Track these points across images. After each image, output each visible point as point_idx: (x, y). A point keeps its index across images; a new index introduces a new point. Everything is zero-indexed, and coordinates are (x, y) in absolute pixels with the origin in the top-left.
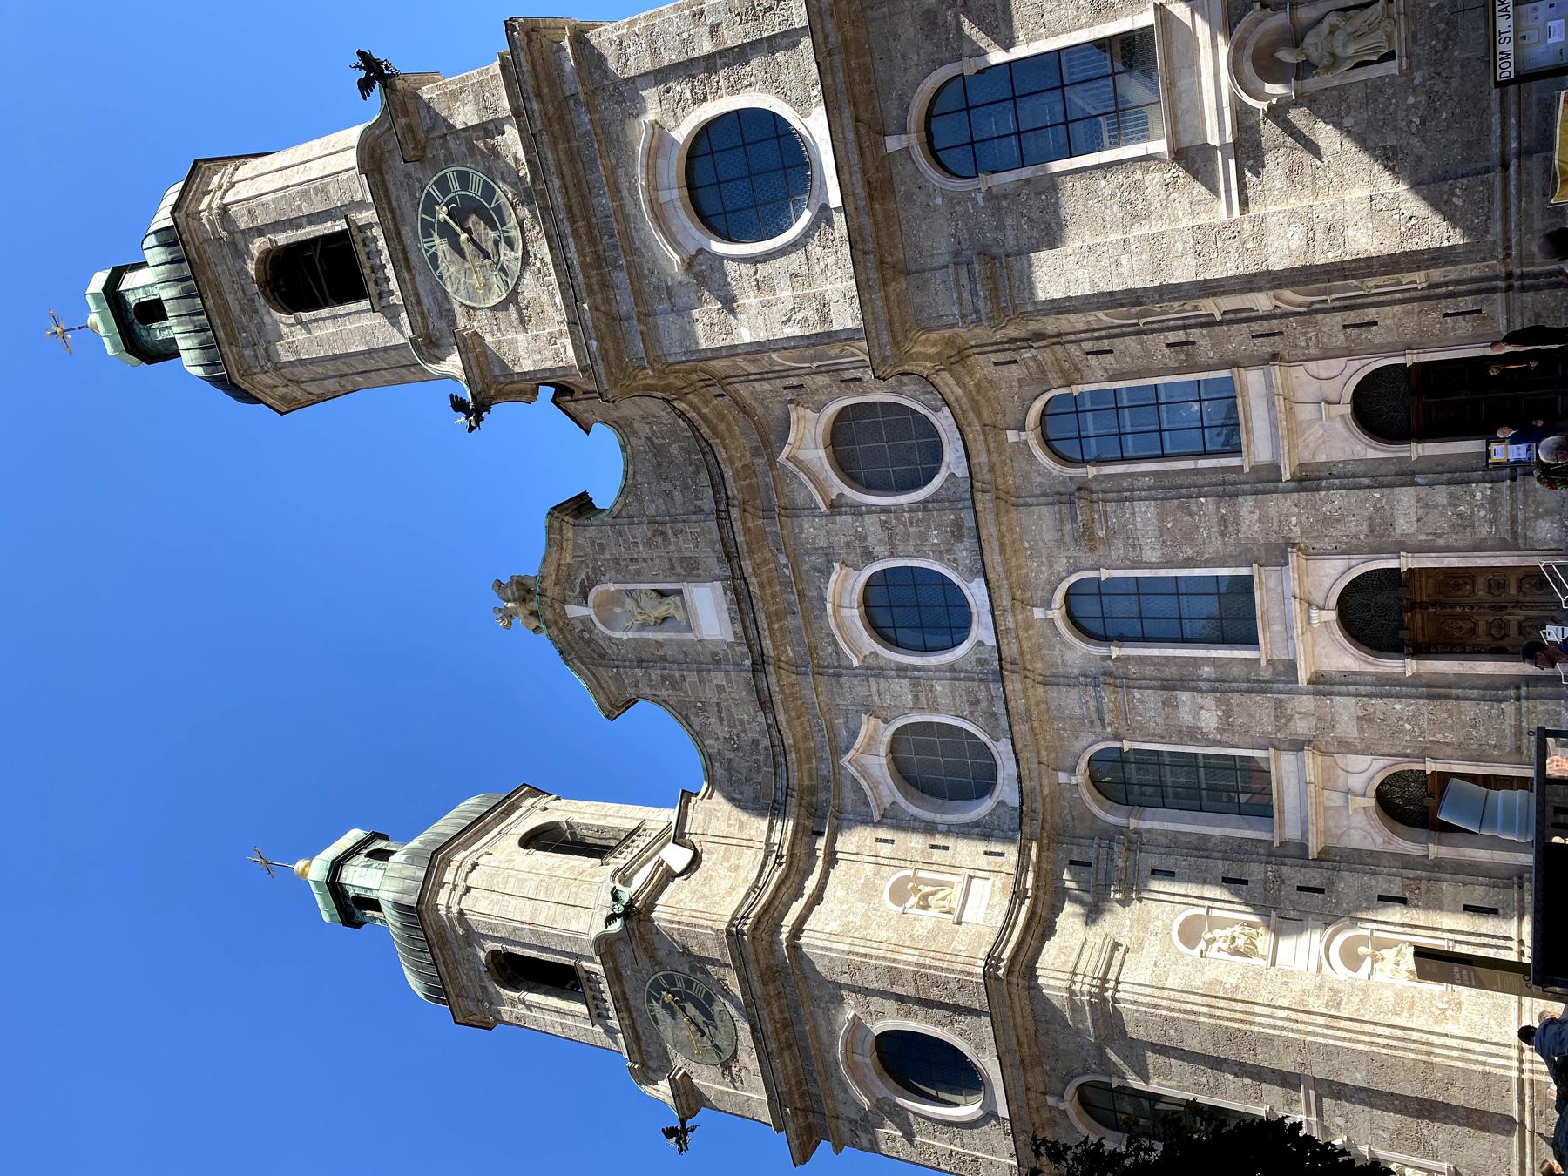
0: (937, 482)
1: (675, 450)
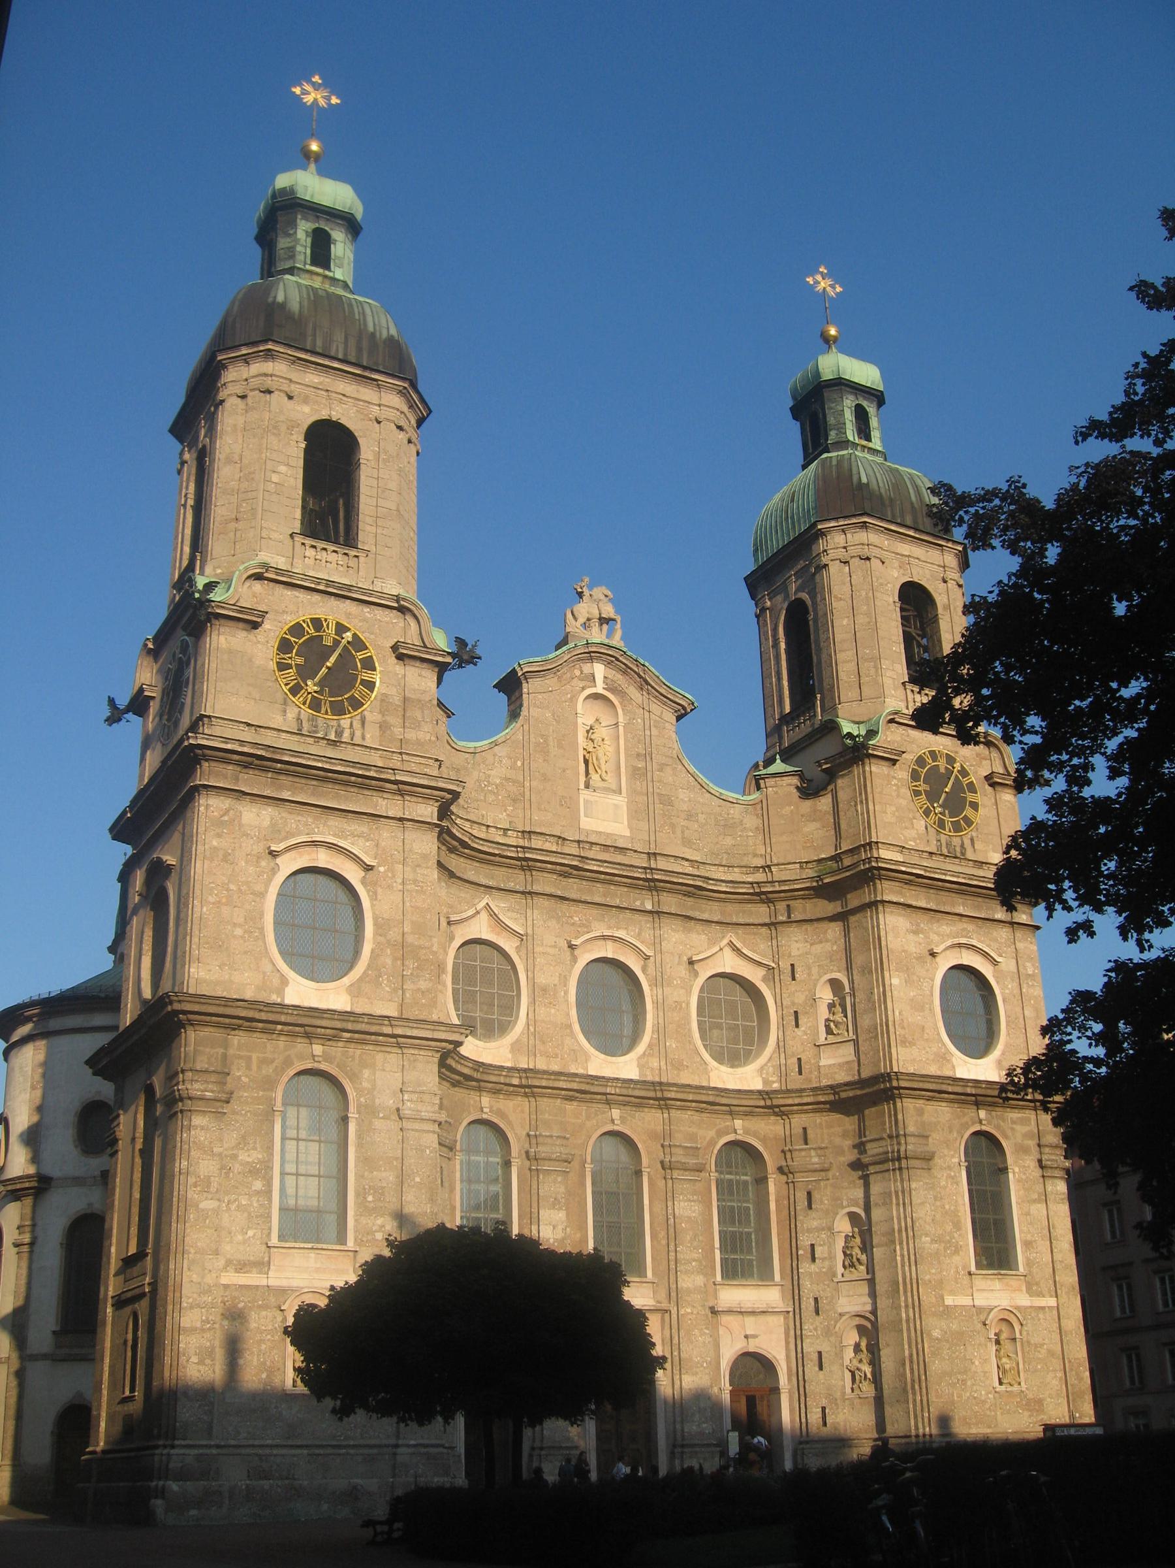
0: (706, 1056)
1: (729, 841)
